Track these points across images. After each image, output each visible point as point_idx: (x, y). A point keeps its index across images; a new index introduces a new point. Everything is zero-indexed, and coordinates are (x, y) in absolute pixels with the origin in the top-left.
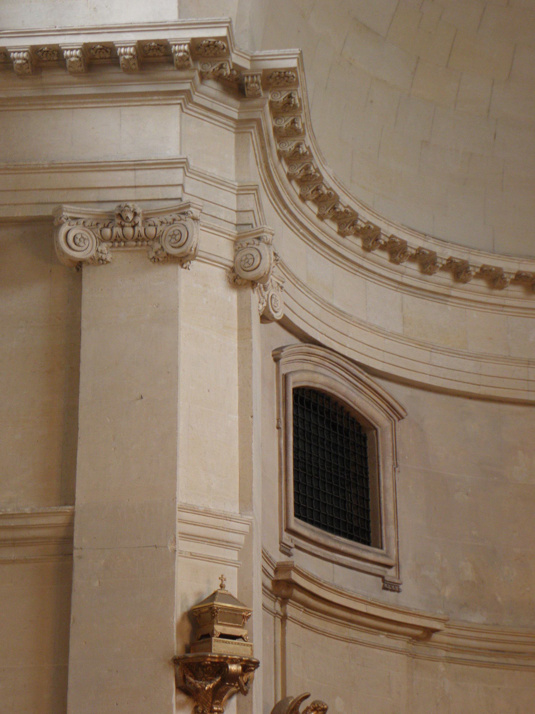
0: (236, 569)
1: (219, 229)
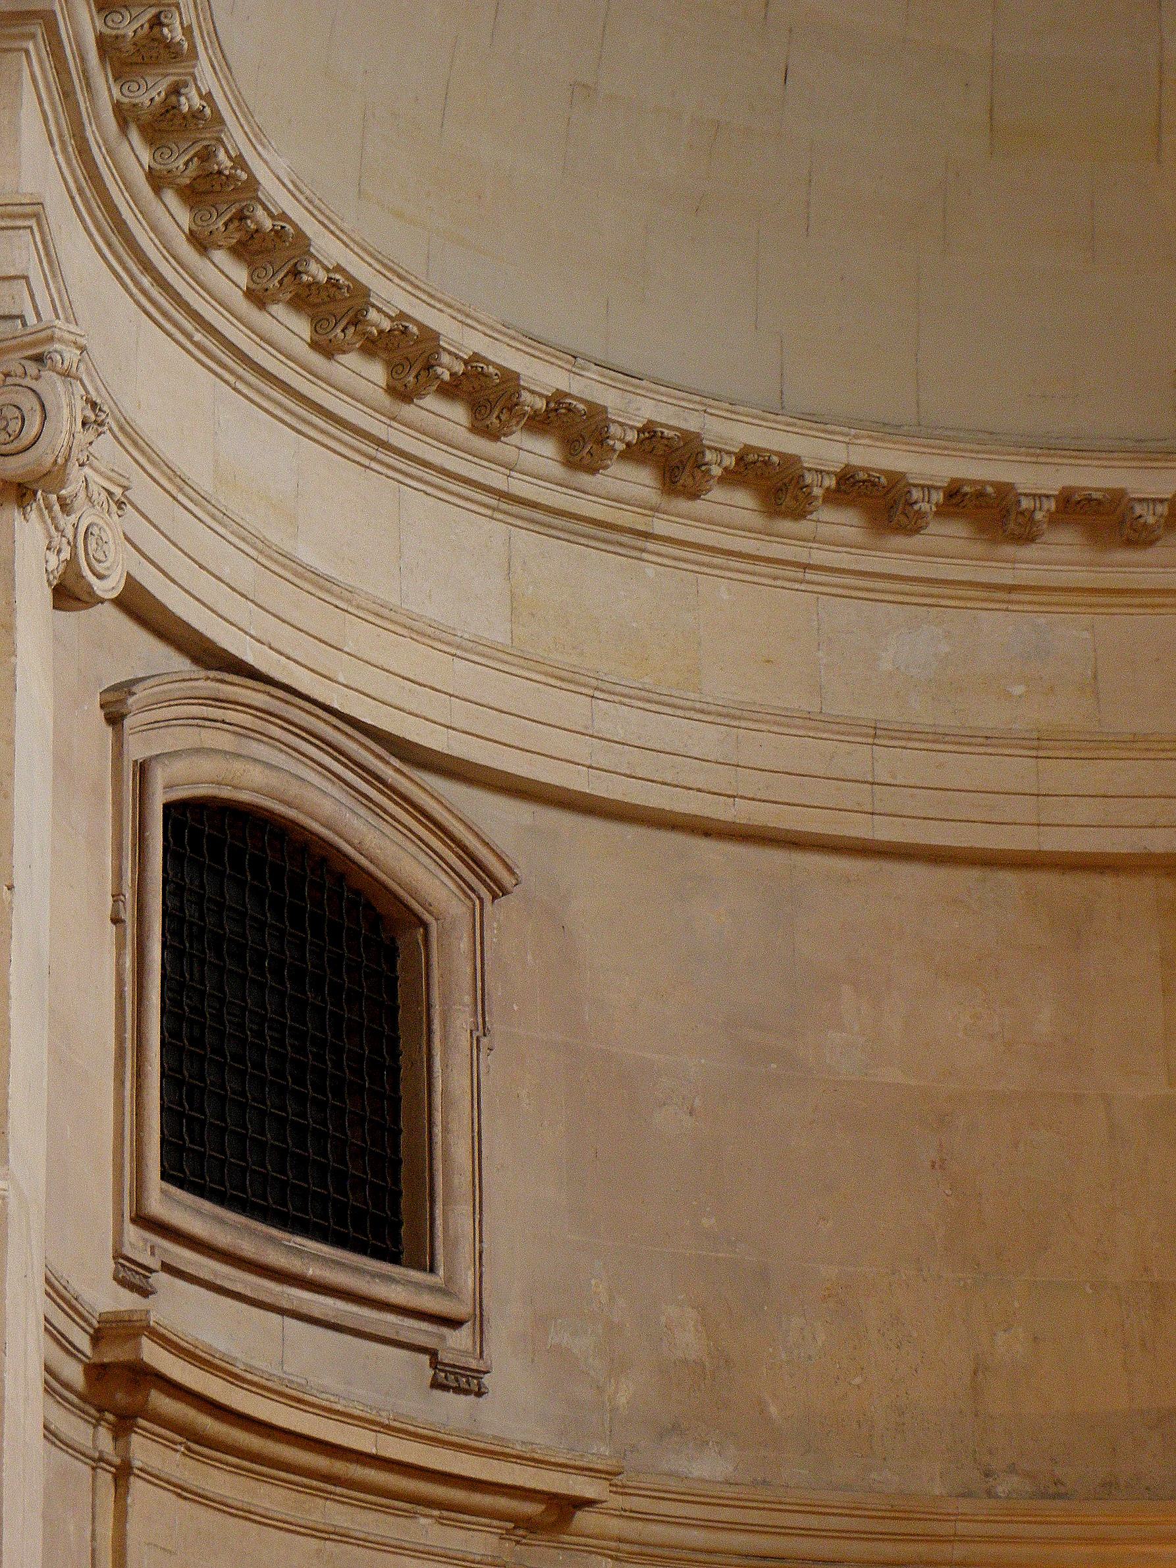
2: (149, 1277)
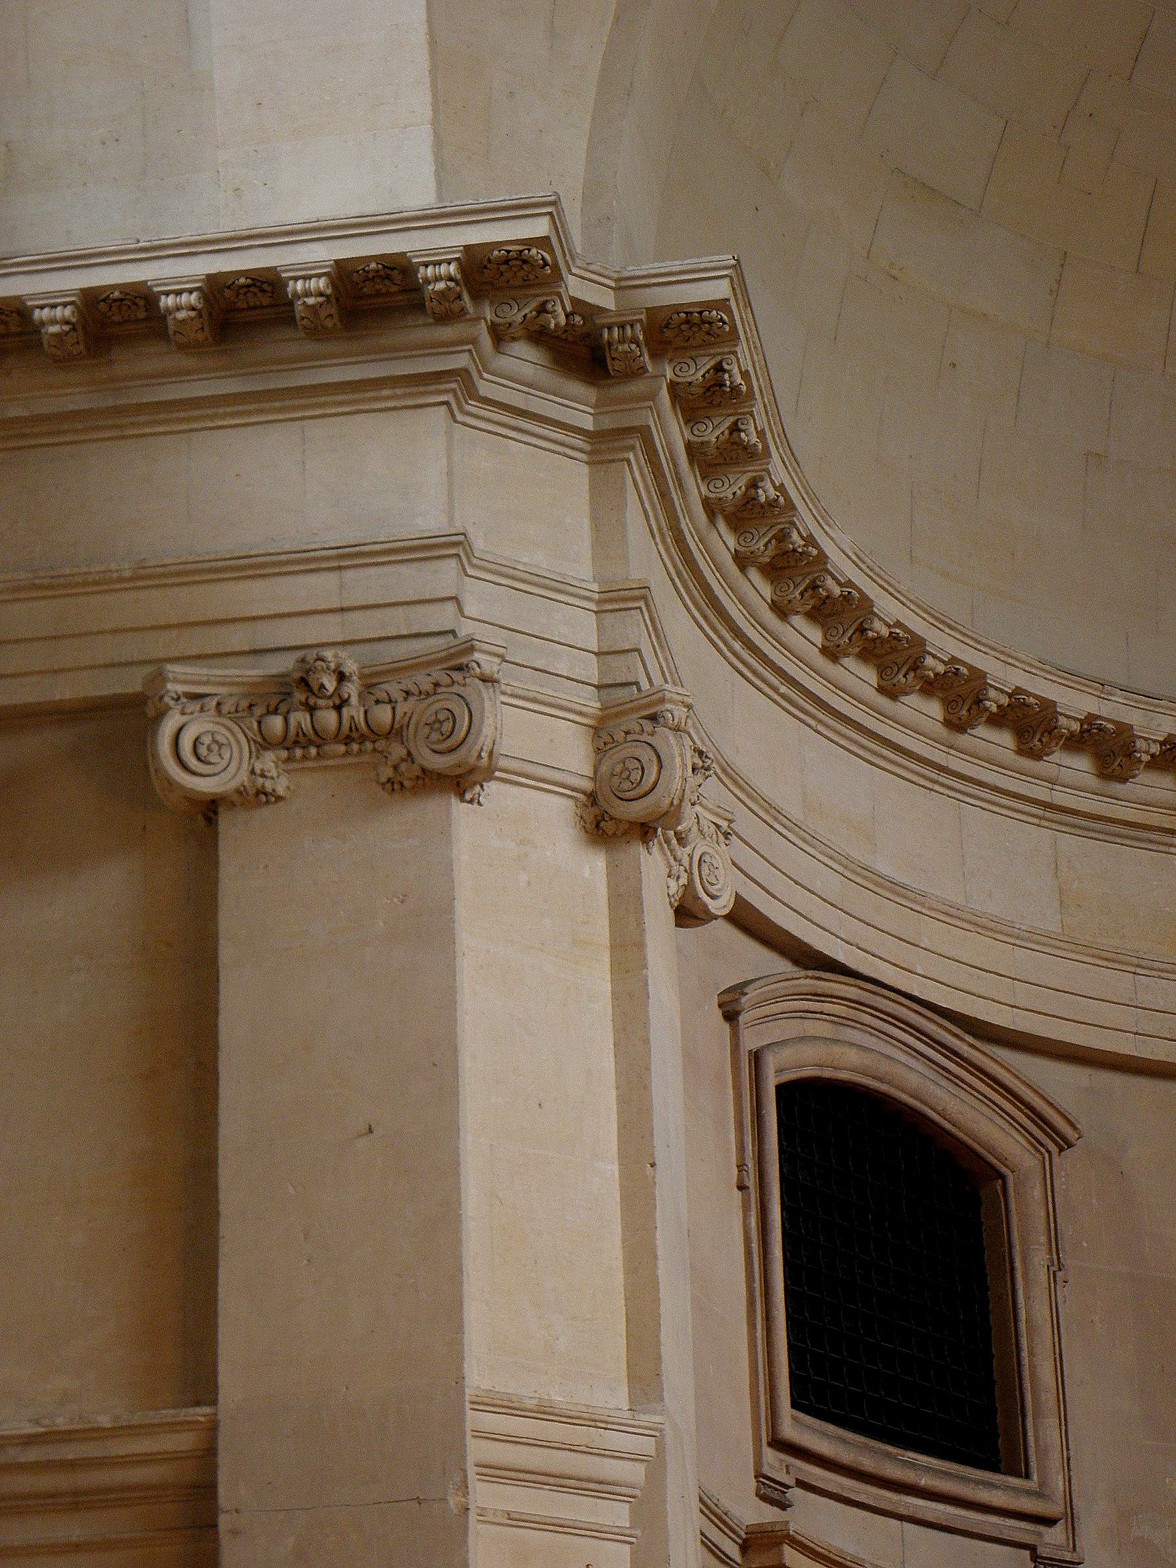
0: (627, 1547)
1: (552, 700)
2: (786, 1493)
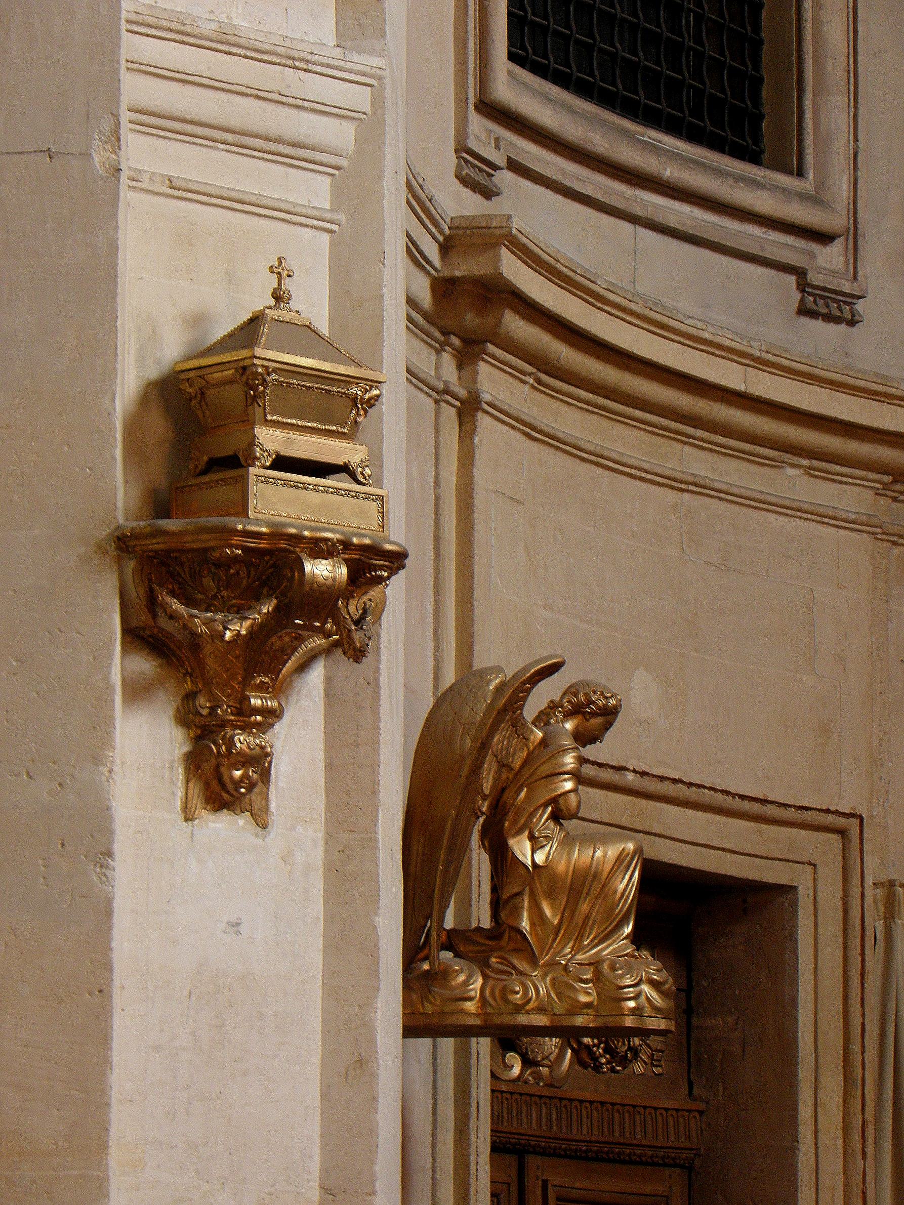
0: (326, 237)
2: (493, 175)
